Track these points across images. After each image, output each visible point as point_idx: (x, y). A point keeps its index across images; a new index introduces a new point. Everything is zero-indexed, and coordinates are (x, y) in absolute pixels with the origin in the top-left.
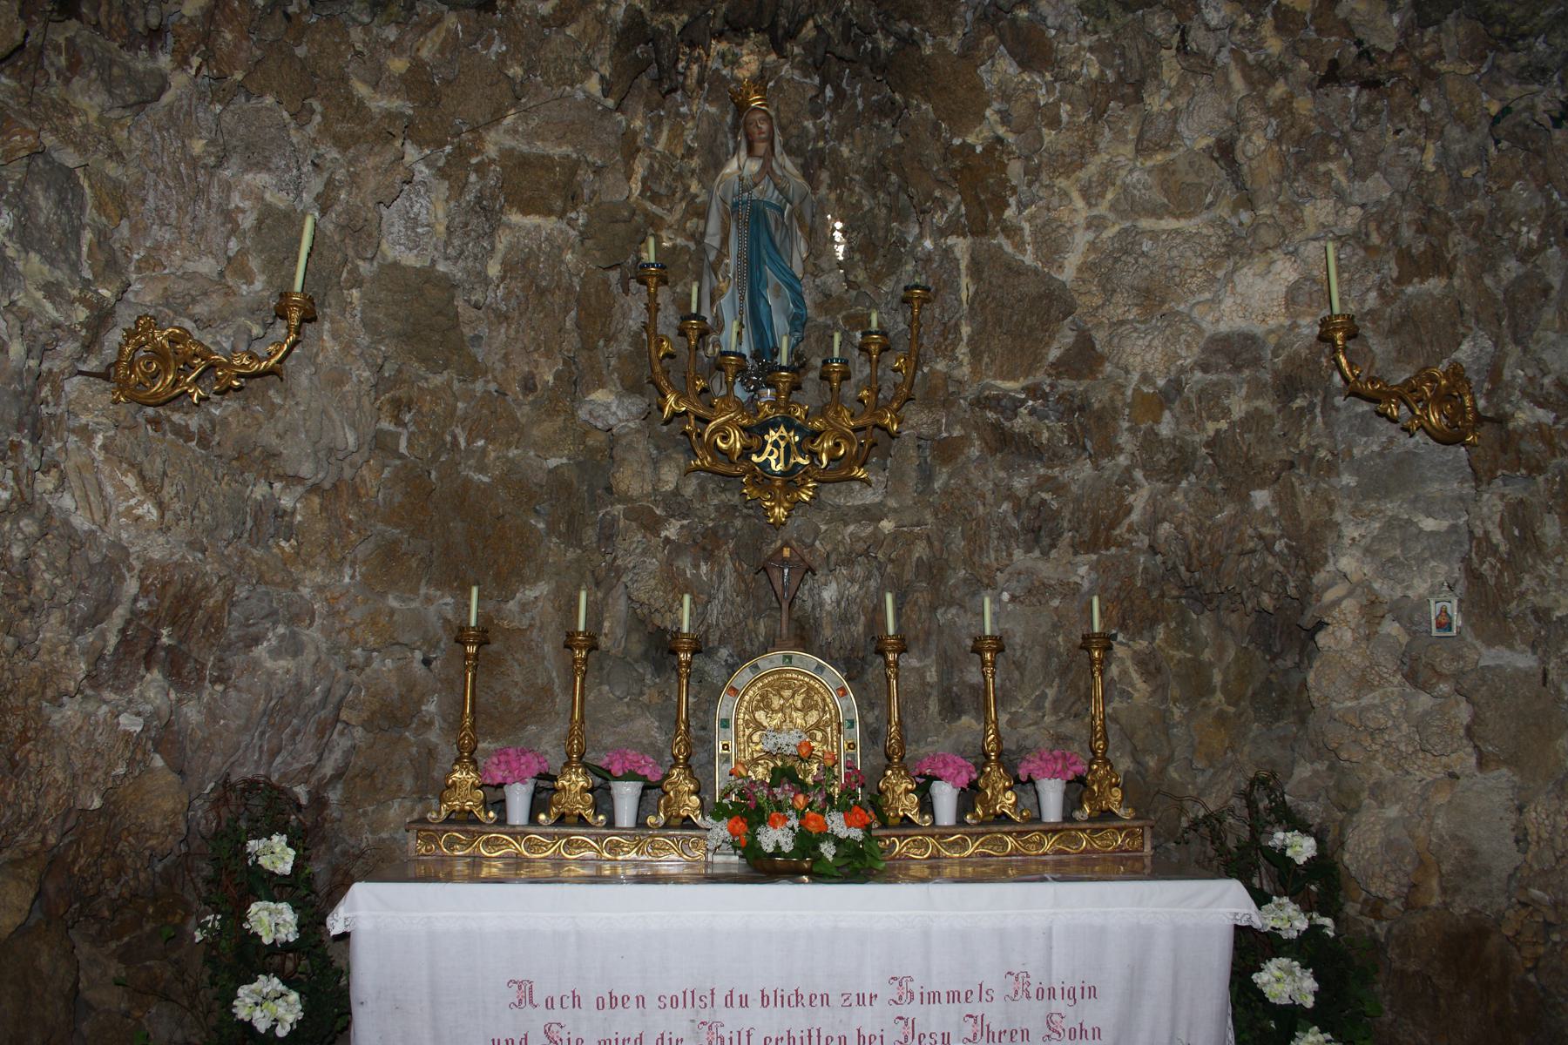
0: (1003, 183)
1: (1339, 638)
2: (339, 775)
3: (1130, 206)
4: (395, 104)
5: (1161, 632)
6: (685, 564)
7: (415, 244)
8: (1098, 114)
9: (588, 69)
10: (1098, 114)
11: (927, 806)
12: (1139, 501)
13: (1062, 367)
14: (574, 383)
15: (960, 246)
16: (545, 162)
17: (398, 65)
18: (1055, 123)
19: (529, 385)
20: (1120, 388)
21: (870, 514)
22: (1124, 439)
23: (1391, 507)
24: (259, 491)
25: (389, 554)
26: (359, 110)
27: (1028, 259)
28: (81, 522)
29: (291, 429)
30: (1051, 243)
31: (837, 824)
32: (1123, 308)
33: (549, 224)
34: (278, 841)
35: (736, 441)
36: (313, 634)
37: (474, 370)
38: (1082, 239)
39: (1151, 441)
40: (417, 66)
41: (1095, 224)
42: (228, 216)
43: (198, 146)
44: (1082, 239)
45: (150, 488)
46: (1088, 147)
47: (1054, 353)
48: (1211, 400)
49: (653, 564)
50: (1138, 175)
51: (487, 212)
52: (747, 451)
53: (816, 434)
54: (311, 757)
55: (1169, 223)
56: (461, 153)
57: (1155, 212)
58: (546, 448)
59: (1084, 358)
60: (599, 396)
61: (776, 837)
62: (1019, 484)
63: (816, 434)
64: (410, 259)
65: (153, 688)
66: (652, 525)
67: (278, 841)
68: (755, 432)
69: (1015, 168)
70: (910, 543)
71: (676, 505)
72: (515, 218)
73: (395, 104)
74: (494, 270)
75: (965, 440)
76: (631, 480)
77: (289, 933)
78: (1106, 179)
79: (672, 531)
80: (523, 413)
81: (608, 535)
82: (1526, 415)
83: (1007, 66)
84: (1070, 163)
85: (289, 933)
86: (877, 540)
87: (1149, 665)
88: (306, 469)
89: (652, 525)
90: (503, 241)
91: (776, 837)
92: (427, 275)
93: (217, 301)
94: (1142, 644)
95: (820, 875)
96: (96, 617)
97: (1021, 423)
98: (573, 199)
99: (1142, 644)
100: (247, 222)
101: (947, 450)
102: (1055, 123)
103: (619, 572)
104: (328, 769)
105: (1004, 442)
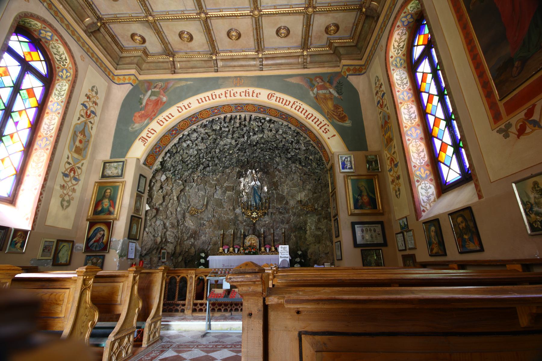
0: (278, 185)
1: (308, 232)
2: (210, 250)
3: (290, 187)
4: (215, 182)
5: (297, 233)
6: (246, 227)
7: (217, 196)
8: (286, 177)
9: (234, 176)
10: (286, 177)
11: (266, 250)
12: (292, 218)
13: (285, 204)
14: (234, 209)
15: (274, 191)
16: (230, 186)
17: (215, 179)
18: (283, 178)
19: (229, 209)
20: (290, 206)
21: (265, 221)
22: (290, 212)
23: (312, 218)
24: (202, 222)
25: (215, 227)
26: (211, 183)
27: (281, 193)
28: (187, 225)
29: (205, 216)
30: (283, 192)
31: (253, 250)
32: (290, 198)
33: (231, 193)
34: (203, 254)
35: (250, 214)
36: (207, 235)
37: (224, 208)
38: (286, 190)
39: (293, 212)
40: (217, 178)
41: (287, 189)
42: (199, 196)
43: (196, 190)
44: (286, 190)
45: (192, 222)
46: (286, 181)
47: (284, 203)
48: (297, 208)
49: (243, 227)
50: (290, 183)
51: (225, 192)
52: (251, 215)
53: (258, 213)
54: (207, 248)
55: (294, 189)
56: (222, 186)
57: (293, 187)
58: (231, 216)
59: (287, 203)
60: (237, 210)
61: (247, 251)
62: (281, 217)
63: (258, 213)
64: (217, 197)
65: (192, 240)
66: (242, 223)
67: (203, 254)
68: (252, 214)
69: (279, 183)
70: (270, 224)
71: (245, 221)
72: (227, 192)
73: (215, 182)
74: (225, 198)
75: (276, 212)
76: (240, 219)
77: (204, 262)
78: (288, 184)
79: (244, 224)
80: (229, 212)
81: (238, 224)
82: (320, 209)
83: (277, 172)
84: (284, 183)
85: (204, 262)
86: (266, 224)
87: (295, 236)
88: (206, 219)
89: (242, 223)
90: (226, 195)
91: (247, 251)
92: (219, 199)
93: (198, 204)
94: (294, 234)
95: (251, 254)
96: (188, 234)
97: (281, 210)
98: (233, 189)
99: (294, 234)
100: (201, 196)
101: (274, 214)
102: (283, 178)
103: (239, 229)
104: (208, 249)
105: (280, 213)
